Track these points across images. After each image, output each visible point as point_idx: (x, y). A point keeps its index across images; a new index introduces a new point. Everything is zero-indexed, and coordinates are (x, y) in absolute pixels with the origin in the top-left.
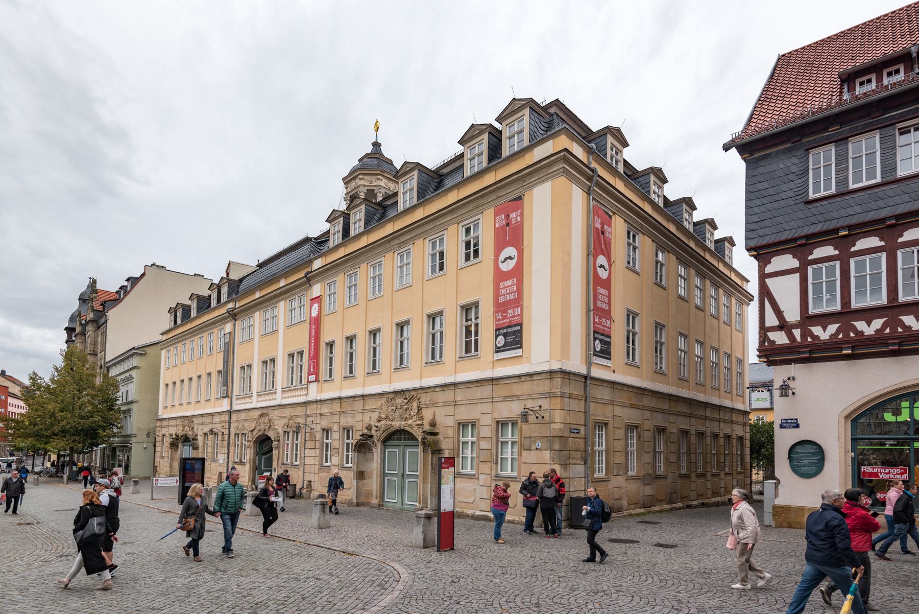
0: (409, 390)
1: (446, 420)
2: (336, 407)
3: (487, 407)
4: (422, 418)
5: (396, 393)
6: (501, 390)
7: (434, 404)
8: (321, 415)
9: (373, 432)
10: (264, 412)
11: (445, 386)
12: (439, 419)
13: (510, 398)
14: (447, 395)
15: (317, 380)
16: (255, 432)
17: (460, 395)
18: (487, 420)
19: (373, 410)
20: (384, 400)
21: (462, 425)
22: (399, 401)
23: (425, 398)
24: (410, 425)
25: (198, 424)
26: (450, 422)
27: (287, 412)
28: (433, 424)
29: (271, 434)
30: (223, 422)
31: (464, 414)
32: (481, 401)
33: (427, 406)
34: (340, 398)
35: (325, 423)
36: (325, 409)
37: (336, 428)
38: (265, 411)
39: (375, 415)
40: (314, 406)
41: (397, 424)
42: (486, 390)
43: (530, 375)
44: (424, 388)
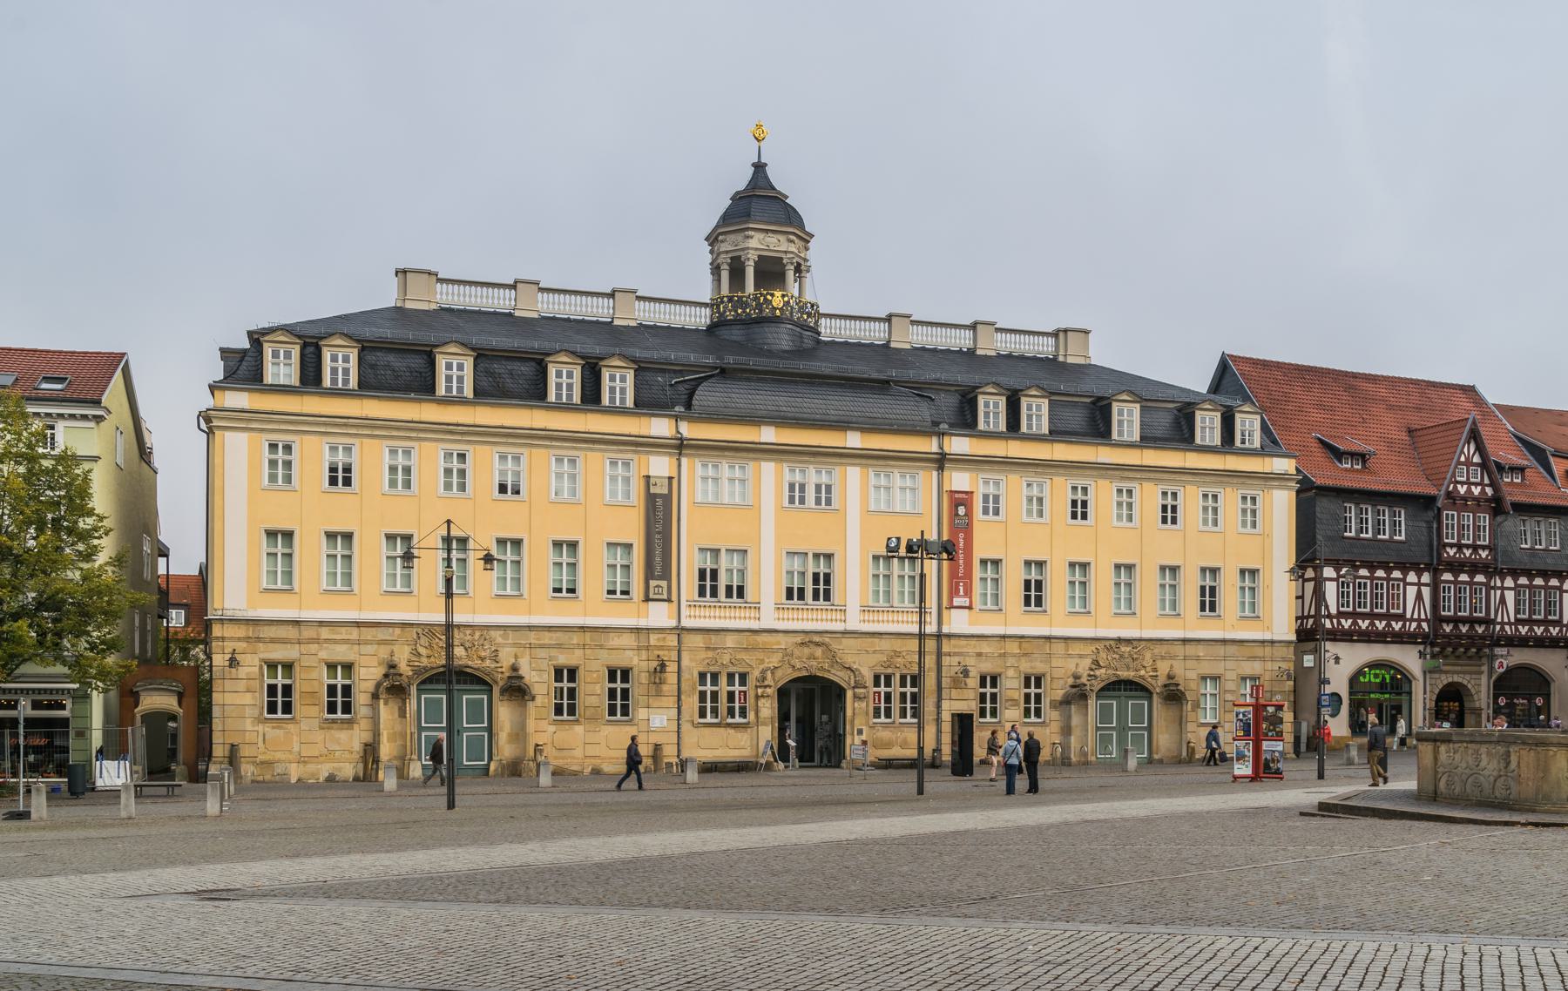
0: (1140, 640)
1: (1188, 675)
2: (1013, 647)
3: (1230, 664)
4: (1155, 670)
5: (1119, 640)
6: (1247, 651)
7: (1171, 658)
8: (979, 655)
9: (1084, 680)
10: (810, 639)
11: (1185, 641)
12: (1179, 669)
13: (1253, 658)
14: (1191, 650)
15: (970, 608)
16: (779, 673)
17: (1201, 651)
18: (1231, 675)
19: (1081, 656)
20: (1100, 646)
21: (1204, 678)
22: (1125, 649)
23: (1159, 650)
24: (1141, 677)
25: (515, 645)
26: (1192, 675)
27: (885, 644)
28: (1170, 677)
29: (838, 676)
30: (661, 648)
31: (1208, 669)
32: (1225, 658)
33: (1163, 658)
34: (1022, 637)
35: (988, 667)
36: (985, 648)
37: (1011, 673)
38: (816, 639)
39: (1087, 662)
40: (963, 642)
41: (1125, 674)
42: (1231, 649)
43: (1272, 642)
44: (1161, 640)
